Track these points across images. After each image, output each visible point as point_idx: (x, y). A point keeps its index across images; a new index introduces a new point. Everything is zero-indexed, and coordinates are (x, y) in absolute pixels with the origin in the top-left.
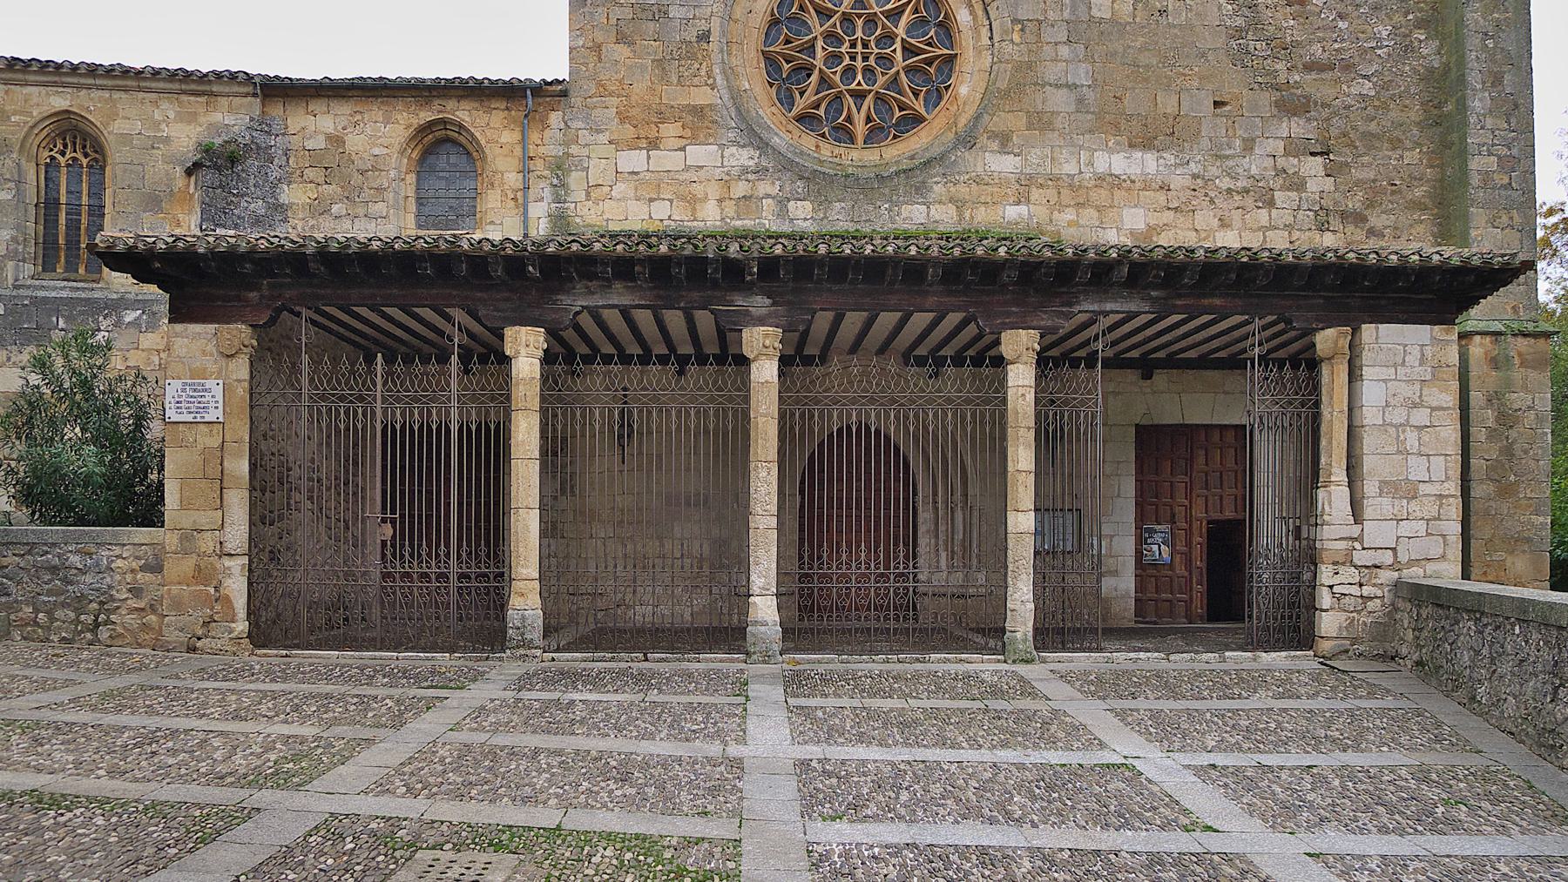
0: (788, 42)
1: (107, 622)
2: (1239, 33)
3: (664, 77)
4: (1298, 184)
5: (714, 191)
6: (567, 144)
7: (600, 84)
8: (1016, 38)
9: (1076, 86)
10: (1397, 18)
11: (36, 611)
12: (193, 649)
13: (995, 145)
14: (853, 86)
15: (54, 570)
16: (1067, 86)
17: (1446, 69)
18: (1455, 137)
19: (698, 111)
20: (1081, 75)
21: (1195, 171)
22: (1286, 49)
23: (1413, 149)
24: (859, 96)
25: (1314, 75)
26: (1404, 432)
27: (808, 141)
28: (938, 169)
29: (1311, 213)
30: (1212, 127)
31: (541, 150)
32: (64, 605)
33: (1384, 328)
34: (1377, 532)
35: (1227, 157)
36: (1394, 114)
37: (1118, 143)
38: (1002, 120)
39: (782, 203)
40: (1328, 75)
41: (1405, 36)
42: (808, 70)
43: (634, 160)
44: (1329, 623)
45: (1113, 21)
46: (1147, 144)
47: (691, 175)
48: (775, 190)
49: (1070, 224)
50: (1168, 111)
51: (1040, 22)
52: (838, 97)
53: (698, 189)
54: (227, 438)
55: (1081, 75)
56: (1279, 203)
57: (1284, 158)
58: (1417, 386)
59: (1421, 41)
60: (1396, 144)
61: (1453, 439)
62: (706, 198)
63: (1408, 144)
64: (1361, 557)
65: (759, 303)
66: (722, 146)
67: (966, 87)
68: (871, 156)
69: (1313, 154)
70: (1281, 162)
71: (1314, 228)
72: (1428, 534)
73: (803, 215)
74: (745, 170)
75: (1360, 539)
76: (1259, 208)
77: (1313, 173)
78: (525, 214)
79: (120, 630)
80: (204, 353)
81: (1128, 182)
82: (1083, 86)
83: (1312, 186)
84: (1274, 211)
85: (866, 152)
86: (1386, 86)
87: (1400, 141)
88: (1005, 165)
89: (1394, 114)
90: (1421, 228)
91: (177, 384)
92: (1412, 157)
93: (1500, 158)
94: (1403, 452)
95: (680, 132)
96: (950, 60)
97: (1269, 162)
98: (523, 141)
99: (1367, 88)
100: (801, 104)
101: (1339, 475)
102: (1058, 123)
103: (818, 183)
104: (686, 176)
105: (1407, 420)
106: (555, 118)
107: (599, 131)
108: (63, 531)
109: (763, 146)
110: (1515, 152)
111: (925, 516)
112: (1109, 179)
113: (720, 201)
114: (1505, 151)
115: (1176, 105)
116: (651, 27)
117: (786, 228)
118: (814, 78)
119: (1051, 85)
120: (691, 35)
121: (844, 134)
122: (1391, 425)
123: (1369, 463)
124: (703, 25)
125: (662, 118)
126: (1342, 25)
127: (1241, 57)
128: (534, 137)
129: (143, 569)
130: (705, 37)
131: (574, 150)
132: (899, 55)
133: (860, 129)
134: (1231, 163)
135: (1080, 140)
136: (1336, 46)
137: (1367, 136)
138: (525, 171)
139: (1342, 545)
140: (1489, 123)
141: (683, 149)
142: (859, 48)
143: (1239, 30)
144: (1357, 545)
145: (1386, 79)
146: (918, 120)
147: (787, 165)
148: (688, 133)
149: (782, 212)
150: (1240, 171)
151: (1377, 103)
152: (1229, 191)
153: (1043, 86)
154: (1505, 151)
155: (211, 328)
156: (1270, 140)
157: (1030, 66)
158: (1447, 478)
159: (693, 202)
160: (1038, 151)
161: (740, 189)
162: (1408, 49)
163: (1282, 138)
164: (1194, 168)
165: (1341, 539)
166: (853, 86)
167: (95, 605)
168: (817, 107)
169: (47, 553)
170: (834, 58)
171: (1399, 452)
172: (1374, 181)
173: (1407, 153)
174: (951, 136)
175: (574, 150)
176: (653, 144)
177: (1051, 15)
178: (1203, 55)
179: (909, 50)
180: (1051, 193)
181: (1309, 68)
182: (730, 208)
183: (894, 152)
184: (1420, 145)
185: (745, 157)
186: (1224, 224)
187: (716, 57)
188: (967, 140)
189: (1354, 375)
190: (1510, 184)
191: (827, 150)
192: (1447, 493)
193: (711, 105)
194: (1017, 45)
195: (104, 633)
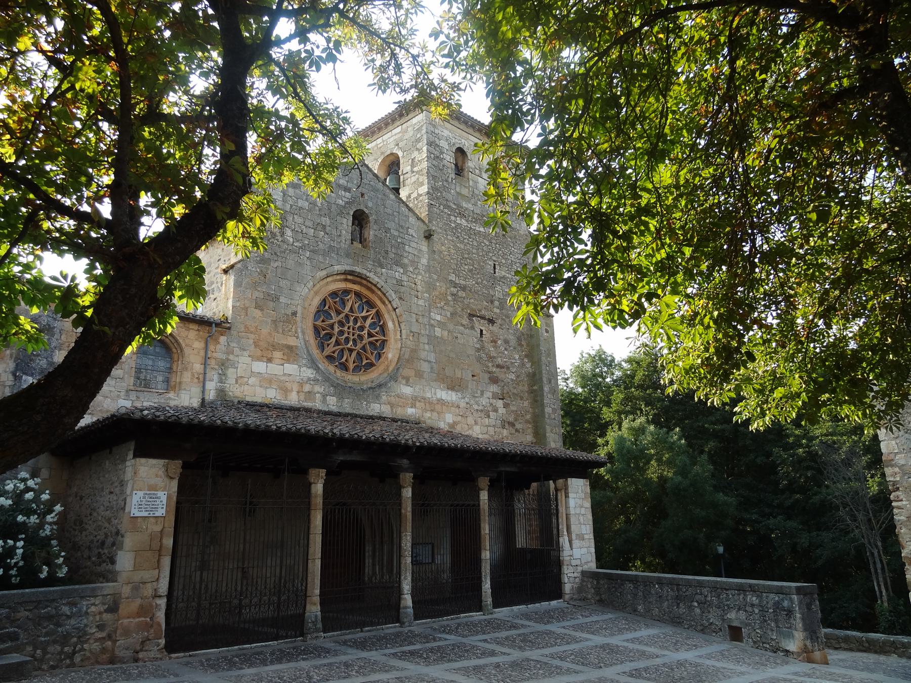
0: (323, 321)
1: (82, 649)
2: (478, 350)
3: (276, 329)
4: (496, 410)
5: (295, 387)
6: (228, 354)
7: (246, 327)
9: (430, 362)
11: (35, 649)
12: (136, 660)
13: (404, 382)
14: (349, 346)
15: (49, 618)
17: (534, 374)
18: (539, 398)
19: (290, 348)
20: (432, 357)
22: (491, 358)
24: (351, 351)
25: (498, 370)
27: (331, 368)
28: (383, 389)
30: (472, 385)
31: (215, 355)
32: (55, 642)
33: (574, 479)
34: (577, 553)
36: (521, 387)
38: (407, 372)
39: (324, 396)
42: (330, 336)
43: (260, 367)
44: (567, 588)
45: (442, 338)
46: (451, 388)
48: (322, 390)
49: (429, 418)
52: (342, 350)
53: (288, 385)
54: (166, 525)
55: (432, 357)
60: (522, 398)
62: (292, 390)
64: (574, 563)
65: (405, 462)
66: (300, 366)
67: (391, 353)
68: (356, 379)
73: (332, 404)
74: (309, 379)
78: (204, 387)
79: (88, 654)
80: (157, 476)
86: (518, 377)
88: (407, 390)
89: (521, 387)
91: (141, 494)
92: (526, 404)
94: (580, 523)
95: (282, 356)
96: (384, 342)
98: (206, 349)
99: (513, 376)
100: (328, 351)
101: (565, 533)
102: (425, 375)
103: (341, 390)
104: (283, 378)
106: (223, 339)
107: (244, 350)
108: (62, 591)
109: (317, 369)
111: (368, 548)
113: (298, 392)
116: (271, 304)
117: (326, 409)
118: (333, 340)
120: (289, 312)
121: (344, 367)
123: (573, 527)
124: (294, 308)
125: (274, 347)
127: (479, 359)
128: (211, 347)
129: (106, 611)
130: (294, 314)
131: (231, 357)
132: (366, 336)
133: (351, 366)
135: (432, 384)
138: (205, 364)
139: (568, 558)
142: (351, 330)
146: (371, 365)
147: (327, 379)
148: (285, 357)
149: (324, 401)
155: (161, 462)
159: (286, 391)
161: (307, 388)
162: (523, 365)
166: (349, 346)
167: (75, 639)
168: (334, 352)
169: (47, 606)
170: (341, 333)
174: (386, 375)
175: (231, 357)
176: (270, 360)
177: (423, 332)
179: (370, 335)
180: (423, 404)
181: (498, 366)
182: (302, 397)
185: (309, 373)
186: (476, 423)
187: (299, 324)
188: (394, 377)
189: (567, 496)
191: (339, 373)
195: (77, 658)
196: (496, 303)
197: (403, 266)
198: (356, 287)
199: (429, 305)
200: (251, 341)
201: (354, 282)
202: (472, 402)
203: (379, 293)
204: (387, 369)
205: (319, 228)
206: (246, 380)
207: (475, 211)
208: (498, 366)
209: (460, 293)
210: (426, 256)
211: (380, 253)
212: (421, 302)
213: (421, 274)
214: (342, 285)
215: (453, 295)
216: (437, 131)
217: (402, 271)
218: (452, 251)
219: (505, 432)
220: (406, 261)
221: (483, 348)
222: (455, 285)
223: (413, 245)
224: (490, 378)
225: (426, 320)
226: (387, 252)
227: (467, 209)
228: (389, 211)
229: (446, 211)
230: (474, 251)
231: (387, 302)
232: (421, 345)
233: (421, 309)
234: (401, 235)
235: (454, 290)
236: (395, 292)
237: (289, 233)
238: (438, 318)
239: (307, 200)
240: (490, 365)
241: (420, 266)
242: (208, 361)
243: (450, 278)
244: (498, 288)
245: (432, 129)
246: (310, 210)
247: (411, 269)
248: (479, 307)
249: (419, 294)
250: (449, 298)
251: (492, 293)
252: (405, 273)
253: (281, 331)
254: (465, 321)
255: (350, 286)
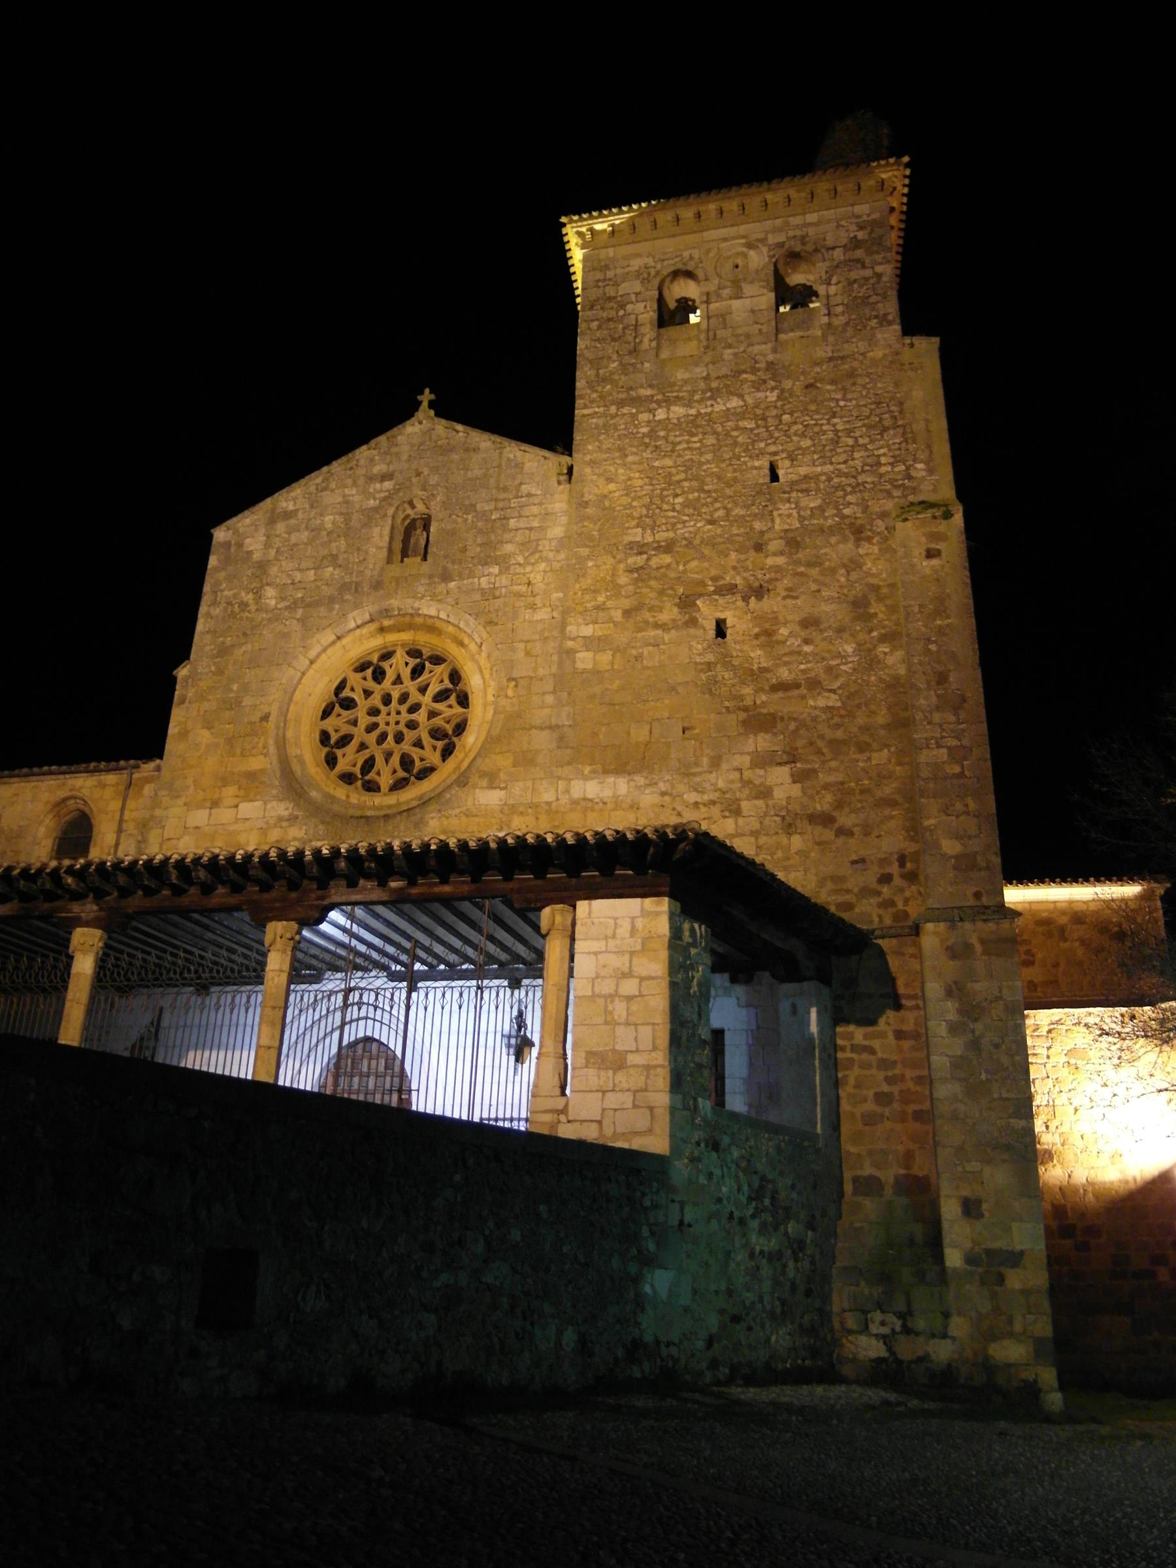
2: (709, 666)
4: (765, 793)
6: (153, 808)
8: (510, 693)
9: (558, 726)
10: (862, 636)
13: (484, 783)
16: (550, 728)
19: (252, 776)
21: (664, 789)
22: (754, 675)
23: (880, 750)
25: (780, 694)
26: (612, 1002)
27: (341, 792)
28: (433, 806)
29: (778, 819)
35: (694, 775)
37: (594, 772)
40: (796, 692)
41: (869, 650)
45: (596, 672)
46: (620, 768)
47: (239, 827)
50: (641, 739)
51: (531, 678)
56: (745, 812)
57: (750, 771)
58: (627, 957)
59: (885, 654)
60: (862, 748)
61: (661, 1008)
63: (875, 745)
66: (265, 804)
68: (389, 800)
69: (780, 764)
70: (747, 774)
71: (780, 831)
72: (635, 1106)
74: (280, 819)
75: (564, 1111)
76: (725, 817)
77: (779, 781)
81: (601, 804)
82: (563, 726)
83: (779, 794)
84: (741, 821)
85: (386, 798)
87: (868, 744)
89: (861, 720)
90: (892, 824)
93: (949, 748)
94: (610, 1022)
97: (735, 776)
99: (833, 701)
104: (232, 828)
105: (616, 991)
107: (178, 797)
110: (965, 742)
112: (583, 803)
114: (955, 743)
115: (647, 733)
116: (227, 714)
119: (536, 728)
120: (256, 717)
121: (371, 787)
122: (599, 996)
124: (265, 709)
125: (224, 782)
126: (807, 649)
127: (710, 688)
128: (131, 804)
130: (265, 718)
131: (158, 812)
134: (698, 779)
135: (559, 772)
136: (802, 667)
137: (836, 745)
140: (937, 717)
141: (237, 806)
143: (709, 664)
144: (563, 1118)
145: (852, 690)
148: (242, 793)
150: (707, 785)
151: (843, 712)
152: (696, 804)
153: (530, 729)
154: (955, 743)
156: (736, 756)
157: (519, 715)
158: (655, 1048)
160: (521, 784)
163: (748, 753)
164: (662, 786)
165: (546, 1111)
171: (606, 1023)
172: (842, 783)
173: (874, 755)
175: (158, 812)
176: (215, 804)
177: (541, 672)
178: (673, 689)
183: (409, 795)
184: (888, 746)
185: (282, 809)
188: (462, 781)
190: (963, 773)
192: (655, 1063)
193: (262, 771)
194: (511, 698)
196: (775, 545)
197: (504, 563)
198: (406, 636)
199: (565, 613)
200: (190, 781)
201: (398, 629)
202: (681, 788)
203: (451, 629)
204: (458, 768)
205: (326, 562)
206: (174, 842)
207: (714, 375)
208: (782, 687)
209: (654, 562)
210: (564, 520)
211: (446, 557)
212: (542, 614)
213: (547, 560)
214: (377, 642)
215: (631, 571)
216: (610, 274)
217: (495, 570)
218: (640, 483)
219: (797, 842)
220: (509, 548)
221: (725, 659)
222: (640, 548)
223: (535, 510)
224: (744, 723)
225: (552, 646)
226: (464, 550)
227: (686, 382)
228: (477, 472)
229: (625, 410)
230: (709, 457)
231: (466, 641)
232: (536, 699)
233: (540, 627)
234: (500, 505)
235: (640, 560)
236: (477, 616)
237: (270, 592)
238: (588, 631)
239: (307, 528)
240: (747, 691)
241: (545, 545)
242: (125, 826)
243: (628, 539)
244: (784, 508)
245: (599, 276)
246: (311, 541)
247: (520, 559)
248: (713, 572)
249: (538, 601)
250: (623, 580)
251: (757, 525)
252: (505, 570)
253: (238, 751)
254: (670, 613)
255: (392, 638)
